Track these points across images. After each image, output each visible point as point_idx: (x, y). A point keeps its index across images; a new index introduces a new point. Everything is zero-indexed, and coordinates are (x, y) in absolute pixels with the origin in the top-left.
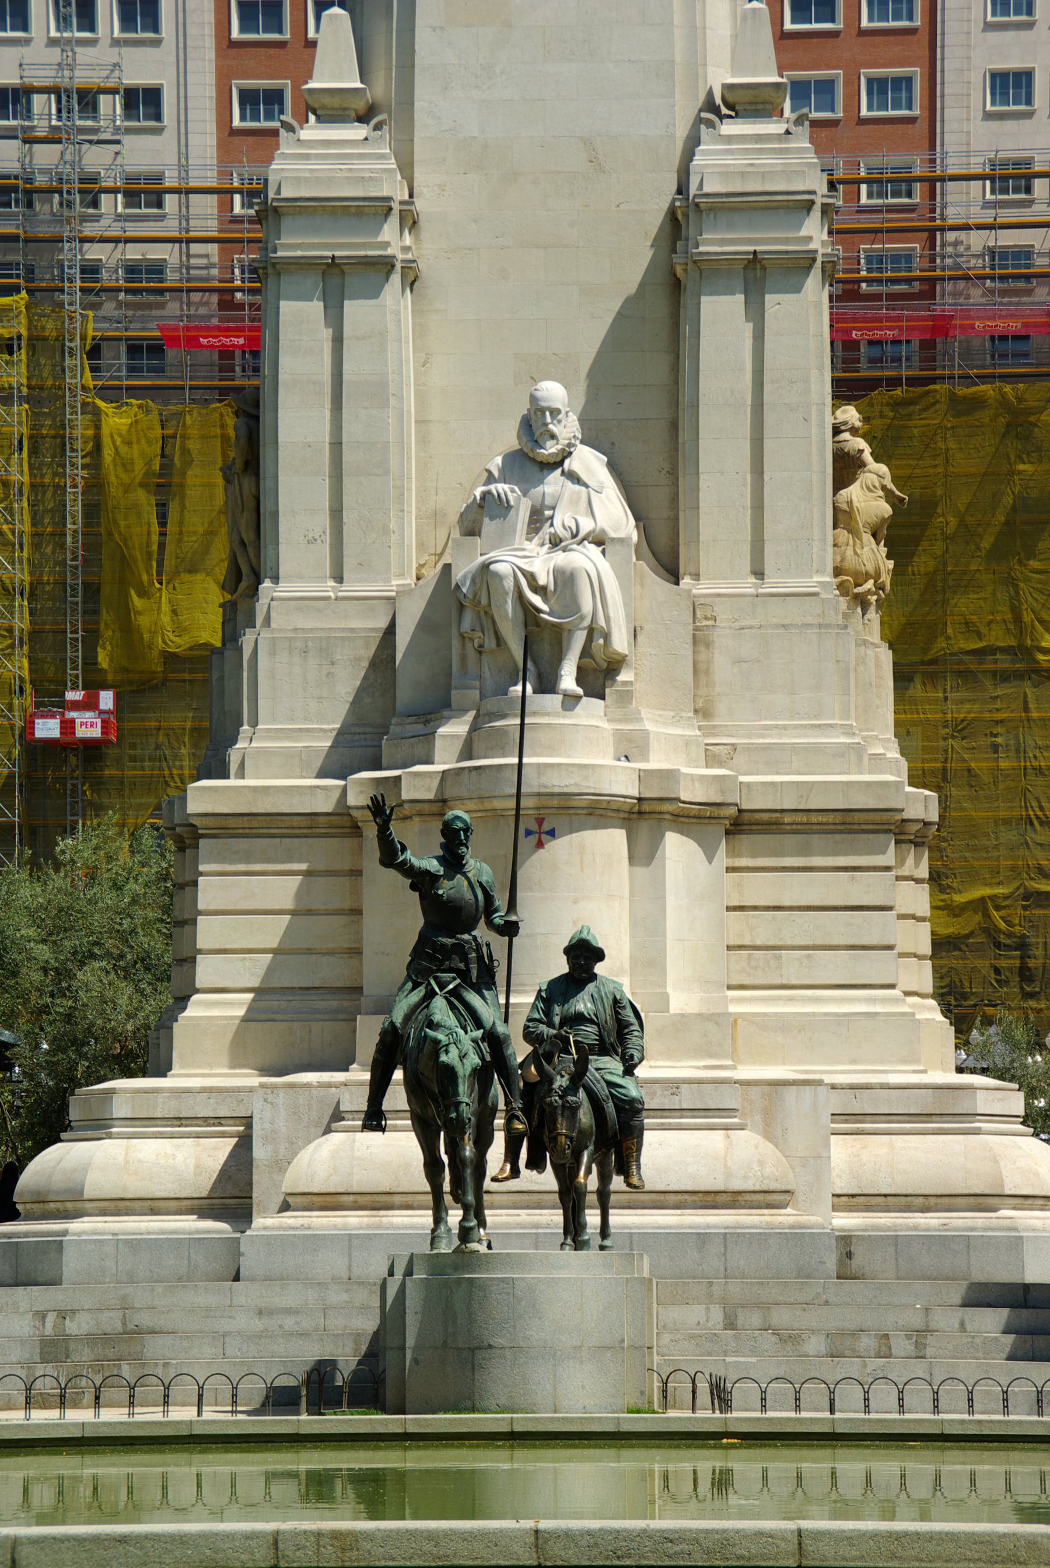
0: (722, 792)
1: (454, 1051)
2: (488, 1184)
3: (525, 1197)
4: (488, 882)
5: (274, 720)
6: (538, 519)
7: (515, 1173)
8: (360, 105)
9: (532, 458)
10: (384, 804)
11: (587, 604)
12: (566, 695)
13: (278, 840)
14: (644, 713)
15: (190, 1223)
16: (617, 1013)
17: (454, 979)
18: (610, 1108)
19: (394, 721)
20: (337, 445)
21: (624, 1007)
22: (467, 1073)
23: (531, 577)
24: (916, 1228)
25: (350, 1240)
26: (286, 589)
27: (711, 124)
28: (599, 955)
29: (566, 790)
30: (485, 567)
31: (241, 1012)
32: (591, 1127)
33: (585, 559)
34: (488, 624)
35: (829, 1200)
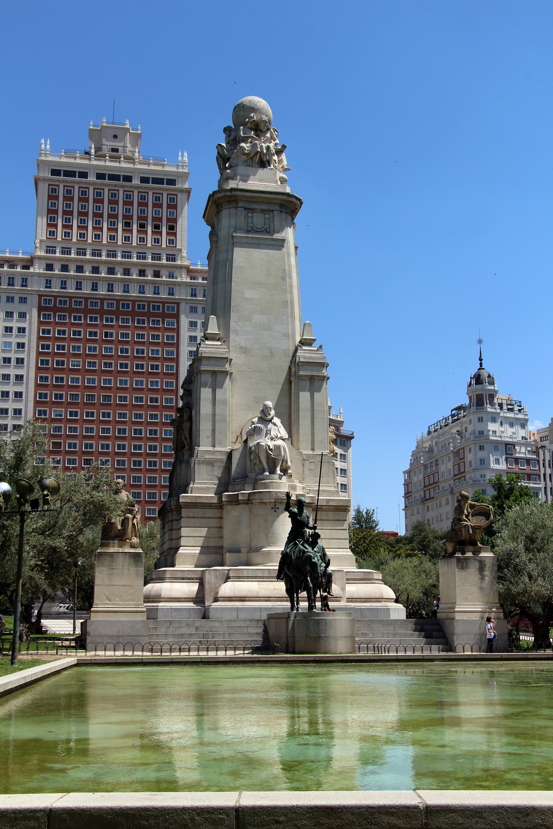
0: (312, 500)
1: (316, 559)
5: (199, 480)
6: (268, 432)
8: (218, 337)
9: (265, 419)
11: (283, 454)
12: (280, 475)
14: (295, 480)
15: (191, 604)
20: (214, 415)
23: (269, 446)
24: (365, 606)
26: (201, 448)
27: (301, 346)
30: (258, 443)
31: (199, 552)
33: (280, 442)
34: (257, 458)
35: (346, 599)
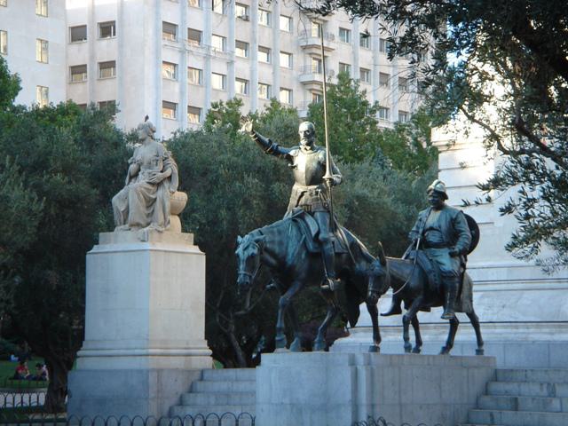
2: (382, 321)
28: (446, 198)
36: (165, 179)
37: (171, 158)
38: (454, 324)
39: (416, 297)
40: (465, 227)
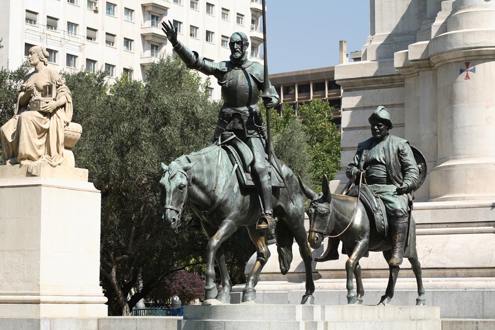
3: (436, 271)
4: (257, 75)
7: (336, 257)
10: (172, 28)
13: (377, 90)
16: (400, 159)
17: (232, 135)
18: (381, 217)
19: (424, 22)
21: (405, 155)
22: (172, 190)
25: (339, 295)
29: (478, 46)
32: (362, 227)
36: (58, 108)
37: (64, 86)
38: (394, 270)
39: (360, 239)
40: (410, 159)
